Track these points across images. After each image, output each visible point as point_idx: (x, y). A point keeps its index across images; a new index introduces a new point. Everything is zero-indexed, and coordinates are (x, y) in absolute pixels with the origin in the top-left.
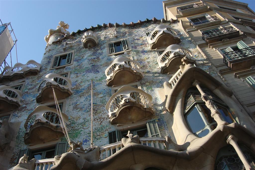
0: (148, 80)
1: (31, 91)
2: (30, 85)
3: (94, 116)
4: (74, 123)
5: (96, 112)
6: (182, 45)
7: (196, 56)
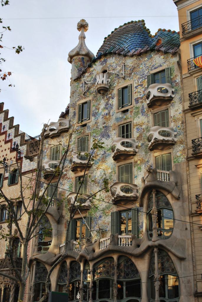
7: (179, 127)
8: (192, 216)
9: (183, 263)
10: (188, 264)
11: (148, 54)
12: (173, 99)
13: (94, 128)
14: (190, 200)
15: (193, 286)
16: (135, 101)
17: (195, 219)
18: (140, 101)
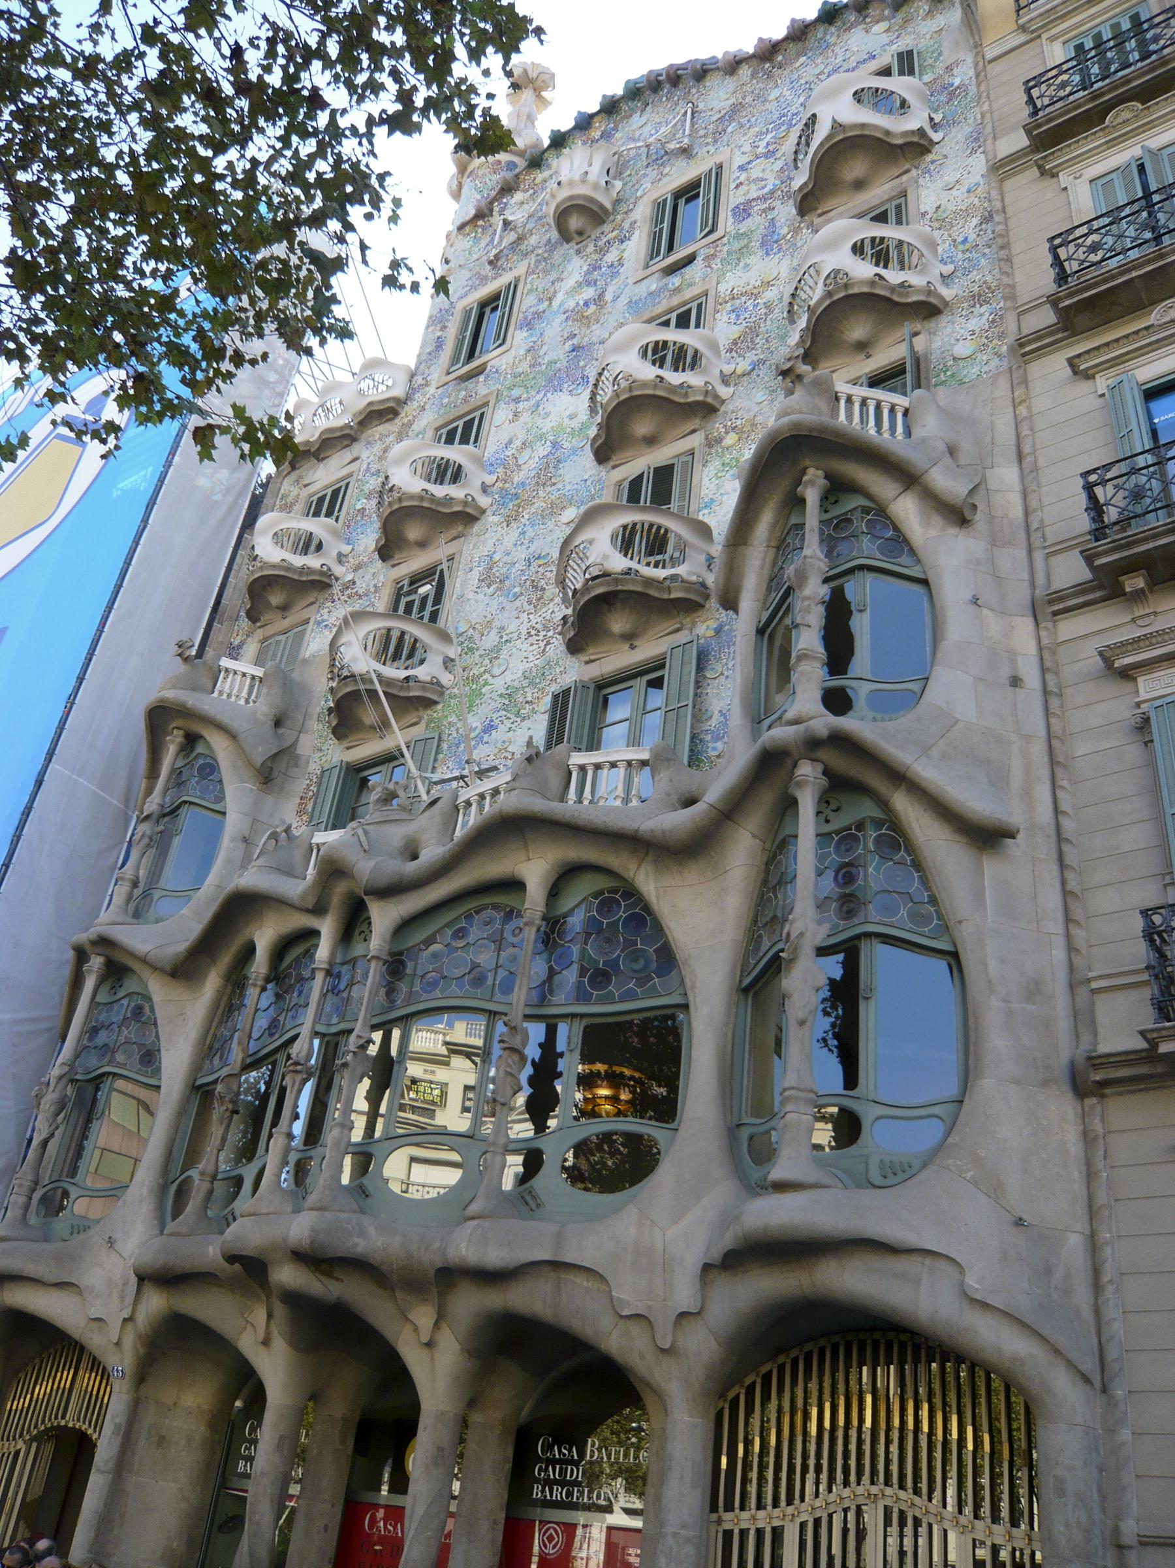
4: (471, 650)
5: (539, 599)
7: (966, 239)
8: (1055, 614)
9: (991, 867)
10: (1024, 869)
11: (812, 42)
14: (1036, 538)
15: (1063, 1023)
17: (1070, 627)
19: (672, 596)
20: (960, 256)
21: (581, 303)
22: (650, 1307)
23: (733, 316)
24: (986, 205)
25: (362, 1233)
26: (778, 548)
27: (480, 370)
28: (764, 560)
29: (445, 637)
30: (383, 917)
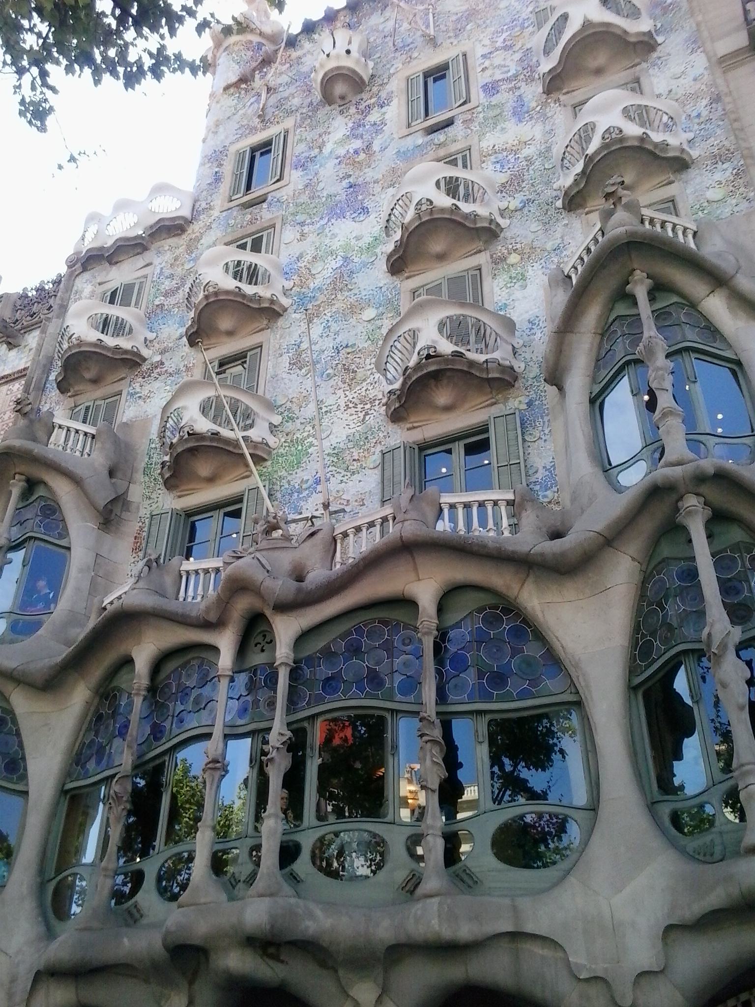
0: (518, 240)
1: (172, 300)
2: (167, 278)
3: (347, 393)
4: (292, 419)
5: (352, 379)
6: (659, 62)
7: (699, 116)
12: (659, 48)
13: (298, 201)
16: (484, 91)
18: (503, 87)
19: (490, 376)
20: (696, 127)
21: (352, 151)
22: (606, 970)
23: (498, 166)
24: (713, 90)
25: (311, 916)
26: (602, 335)
27: (262, 200)
28: (592, 344)
29: (271, 406)
30: (285, 630)
